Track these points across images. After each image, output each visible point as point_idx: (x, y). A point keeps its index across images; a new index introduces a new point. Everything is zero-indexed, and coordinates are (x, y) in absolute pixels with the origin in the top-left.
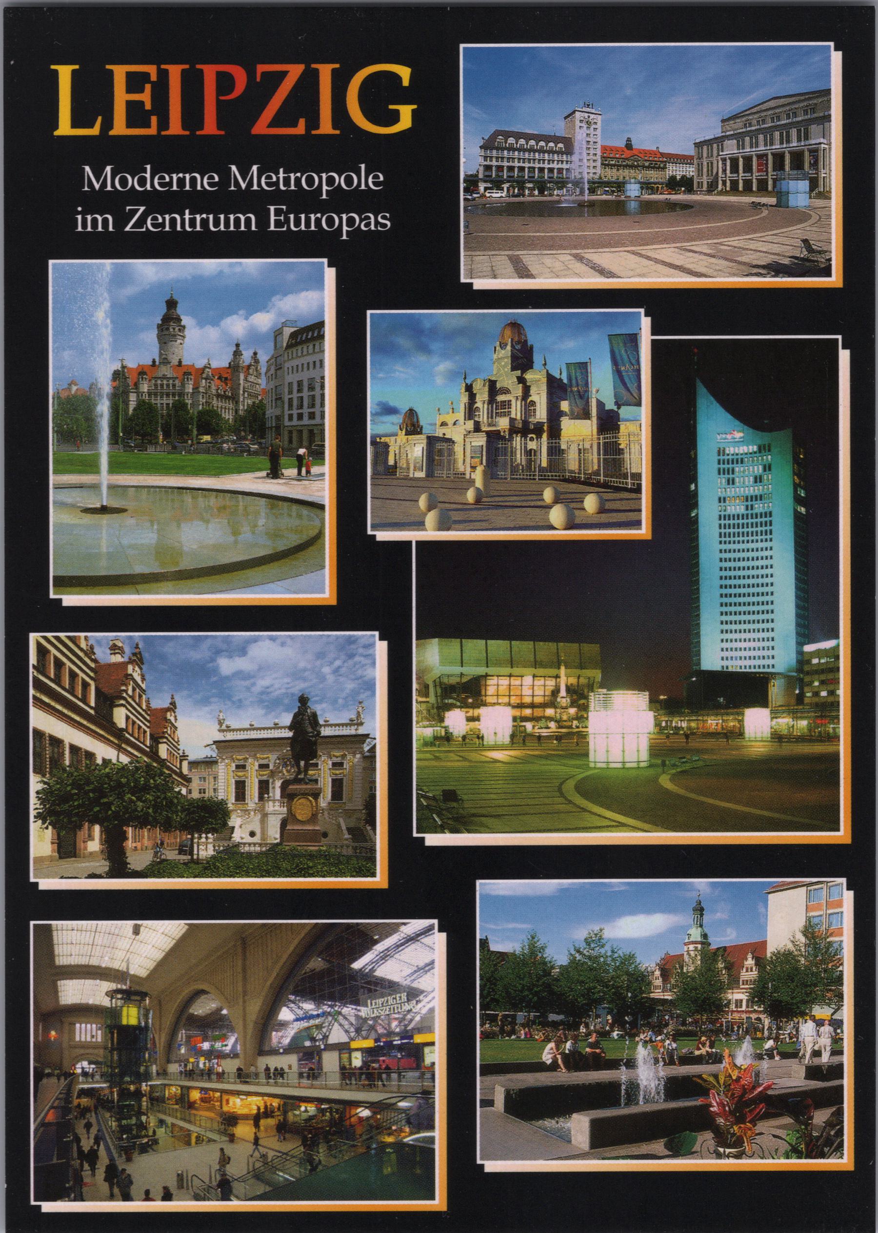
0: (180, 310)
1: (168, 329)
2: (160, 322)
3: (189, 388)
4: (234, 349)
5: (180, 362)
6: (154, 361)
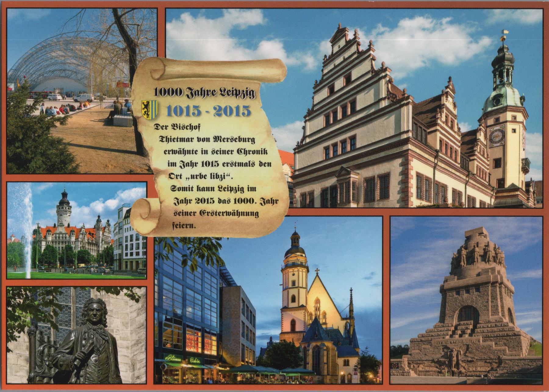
0: (69, 198)
1: (63, 208)
3: (73, 239)
4: (97, 218)
5: (69, 225)
6: (55, 225)
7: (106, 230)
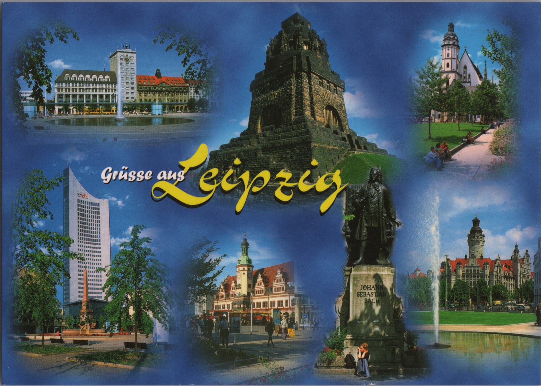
0: (481, 225)
1: (474, 237)
3: (487, 272)
4: (514, 248)
5: (482, 256)
6: (466, 256)
7: (524, 261)
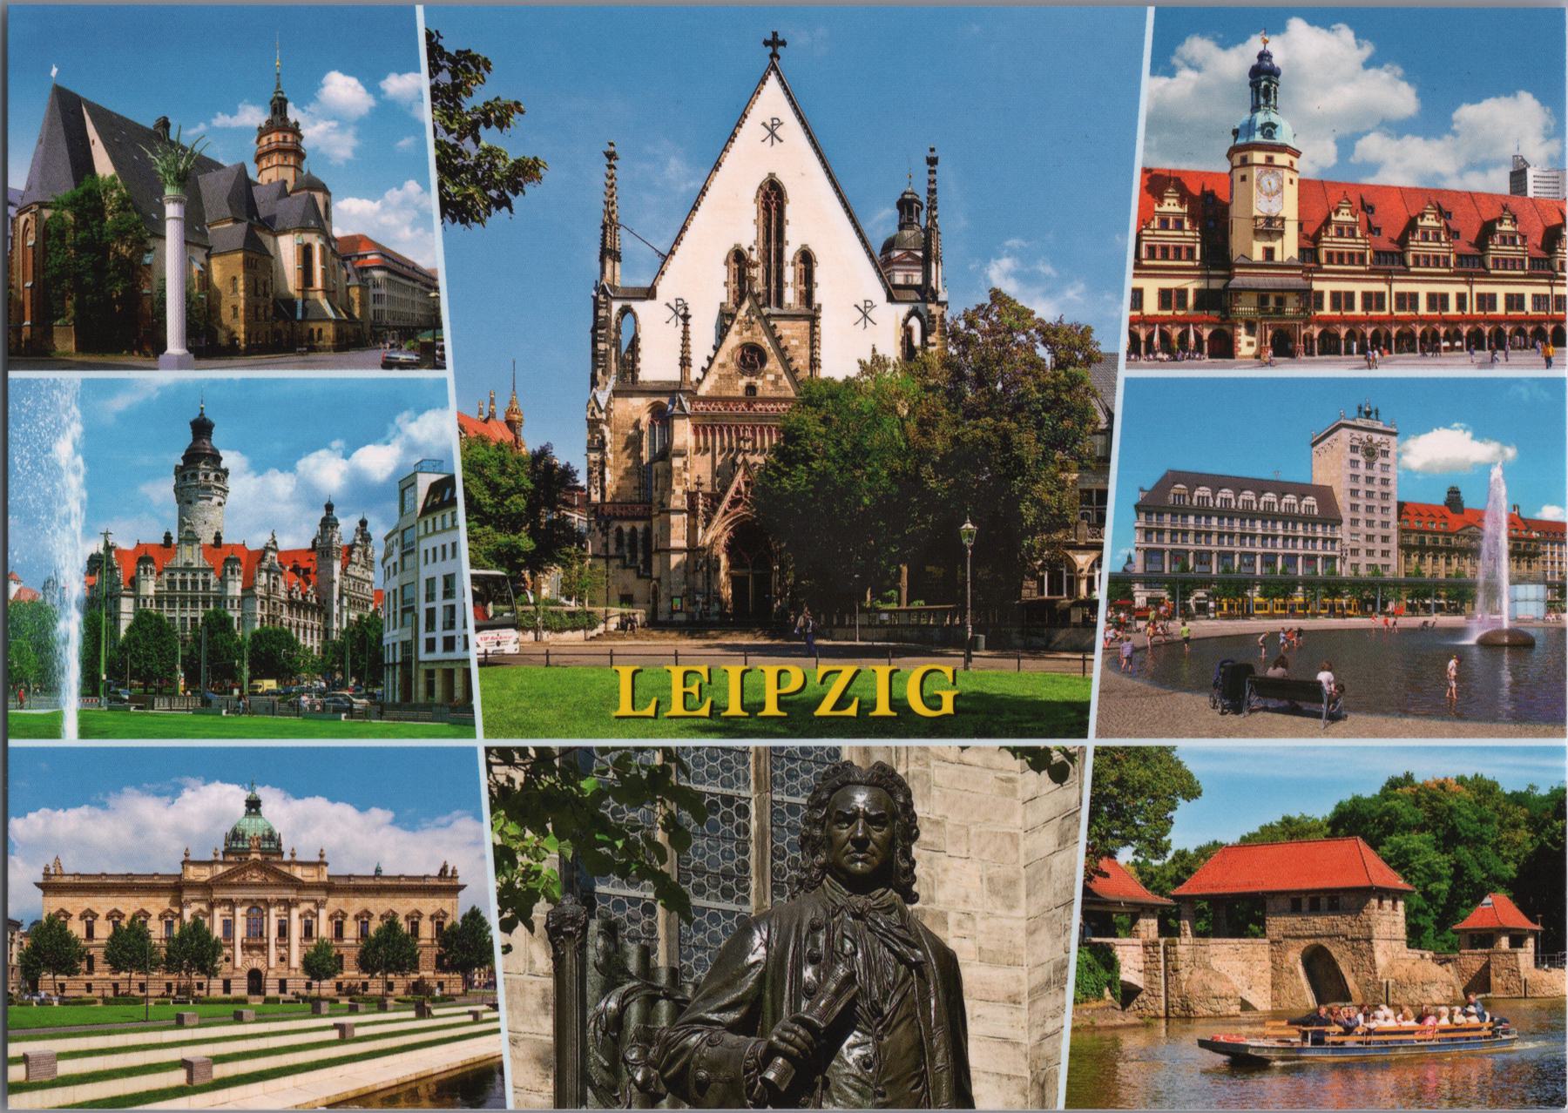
0: (217, 439)
2: (181, 463)
3: (235, 588)
4: (324, 514)
5: (218, 537)
6: (168, 537)
7: (355, 556)
